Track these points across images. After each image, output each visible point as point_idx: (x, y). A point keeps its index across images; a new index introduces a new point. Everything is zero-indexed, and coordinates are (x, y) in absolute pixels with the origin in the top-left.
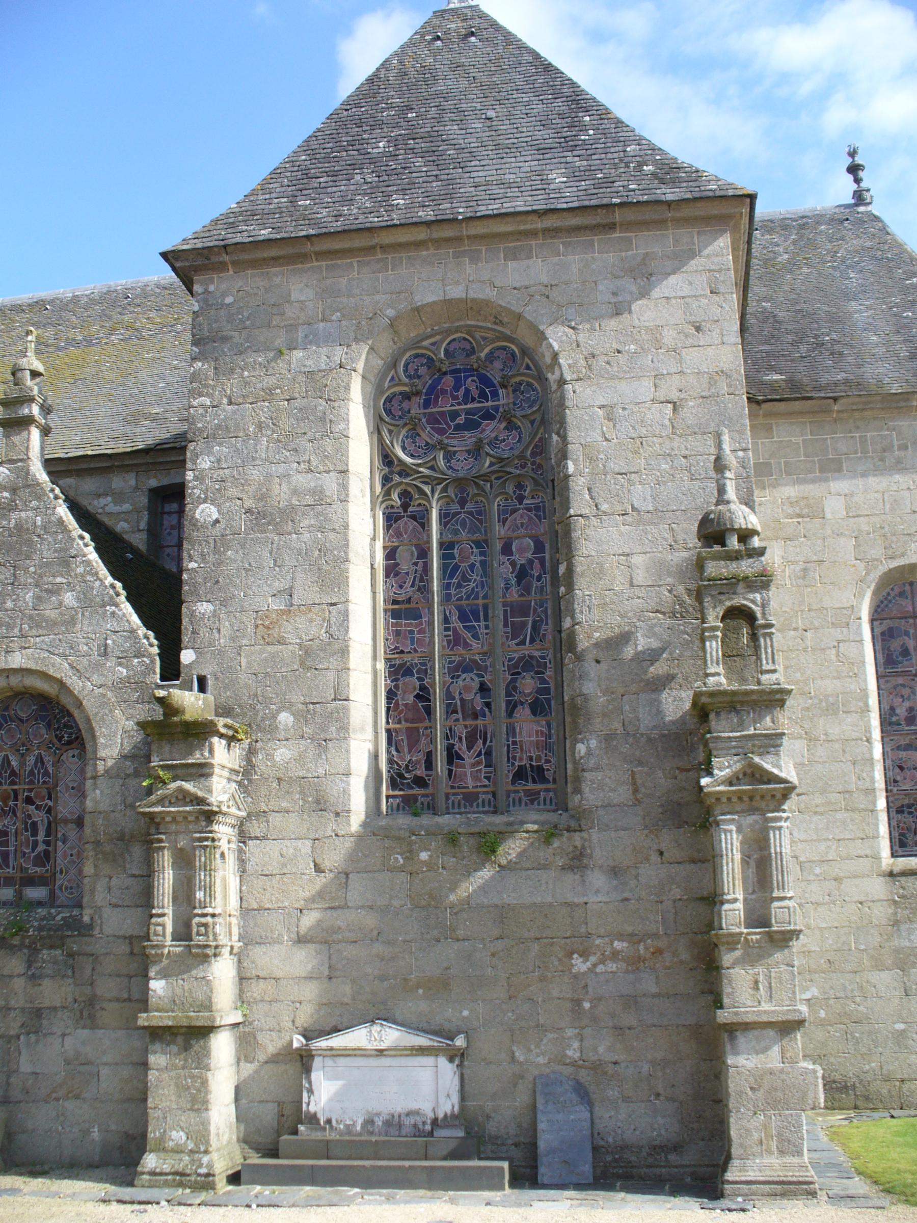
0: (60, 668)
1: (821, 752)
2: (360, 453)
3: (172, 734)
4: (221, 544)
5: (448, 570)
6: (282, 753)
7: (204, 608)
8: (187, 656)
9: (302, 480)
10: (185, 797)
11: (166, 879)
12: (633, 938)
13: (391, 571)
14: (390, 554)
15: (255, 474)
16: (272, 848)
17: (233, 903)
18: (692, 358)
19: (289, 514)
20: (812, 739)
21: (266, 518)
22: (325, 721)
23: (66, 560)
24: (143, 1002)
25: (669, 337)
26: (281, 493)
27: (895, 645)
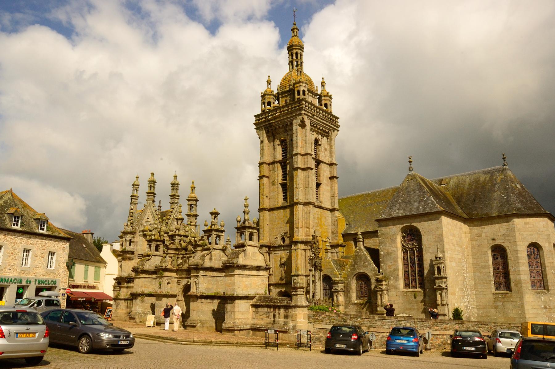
0: (366, 272)
1: (482, 274)
2: (399, 245)
3: (378, 281)
4: (384, 257)
5: (410, 259)
6: (392, 282)
7: (382, 265)
8: (381, 270)
9: (393, 249)
10: (380, 288)
11: (379, 297)
12: (431, 304)
13: (404, 259)
14: (404, 257)
15: (387, 248)
16: (392, 293)
17: (387, 299)
18: (437, 232)
19: (391, 253)
20: (480, 273)
21: (389, 254)
22: (396, 278)
23: (366, 259)
24: (377, 311)
25: (434, 229)
26: (390, 251)
27: (495, 257)
